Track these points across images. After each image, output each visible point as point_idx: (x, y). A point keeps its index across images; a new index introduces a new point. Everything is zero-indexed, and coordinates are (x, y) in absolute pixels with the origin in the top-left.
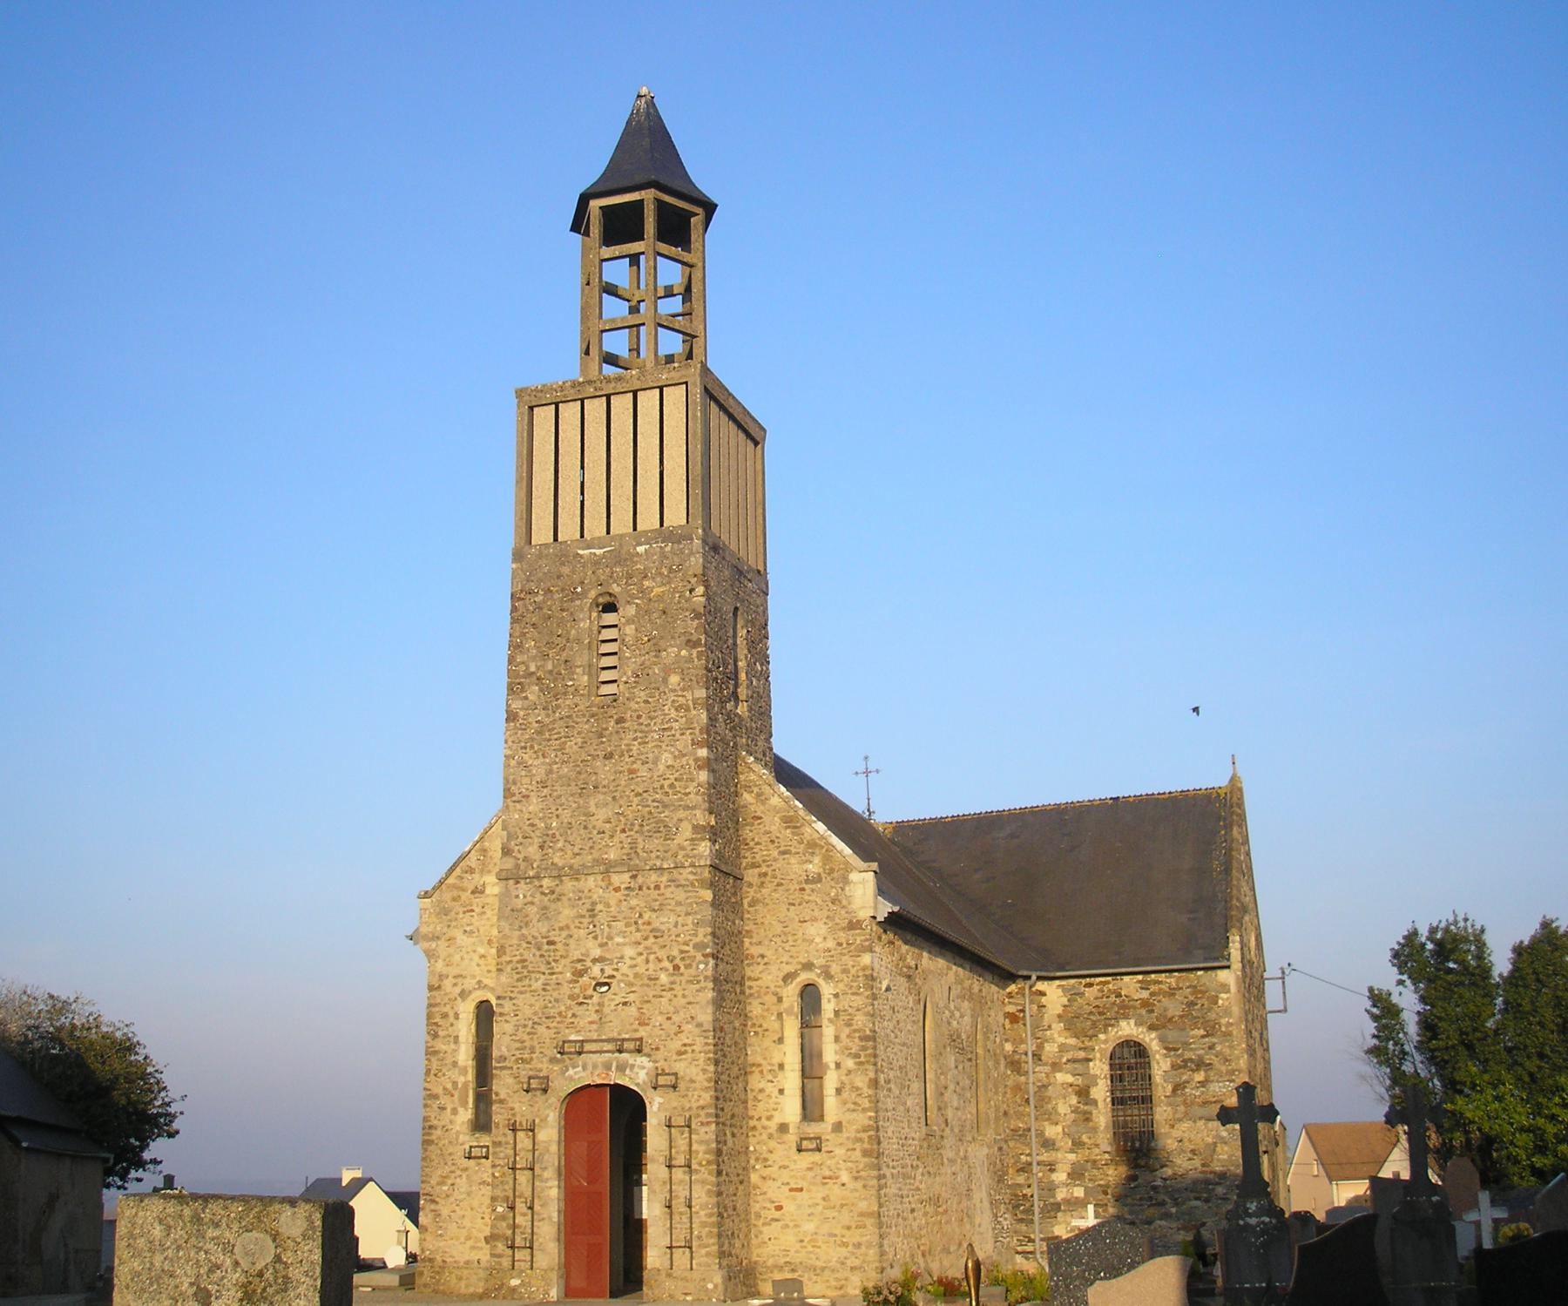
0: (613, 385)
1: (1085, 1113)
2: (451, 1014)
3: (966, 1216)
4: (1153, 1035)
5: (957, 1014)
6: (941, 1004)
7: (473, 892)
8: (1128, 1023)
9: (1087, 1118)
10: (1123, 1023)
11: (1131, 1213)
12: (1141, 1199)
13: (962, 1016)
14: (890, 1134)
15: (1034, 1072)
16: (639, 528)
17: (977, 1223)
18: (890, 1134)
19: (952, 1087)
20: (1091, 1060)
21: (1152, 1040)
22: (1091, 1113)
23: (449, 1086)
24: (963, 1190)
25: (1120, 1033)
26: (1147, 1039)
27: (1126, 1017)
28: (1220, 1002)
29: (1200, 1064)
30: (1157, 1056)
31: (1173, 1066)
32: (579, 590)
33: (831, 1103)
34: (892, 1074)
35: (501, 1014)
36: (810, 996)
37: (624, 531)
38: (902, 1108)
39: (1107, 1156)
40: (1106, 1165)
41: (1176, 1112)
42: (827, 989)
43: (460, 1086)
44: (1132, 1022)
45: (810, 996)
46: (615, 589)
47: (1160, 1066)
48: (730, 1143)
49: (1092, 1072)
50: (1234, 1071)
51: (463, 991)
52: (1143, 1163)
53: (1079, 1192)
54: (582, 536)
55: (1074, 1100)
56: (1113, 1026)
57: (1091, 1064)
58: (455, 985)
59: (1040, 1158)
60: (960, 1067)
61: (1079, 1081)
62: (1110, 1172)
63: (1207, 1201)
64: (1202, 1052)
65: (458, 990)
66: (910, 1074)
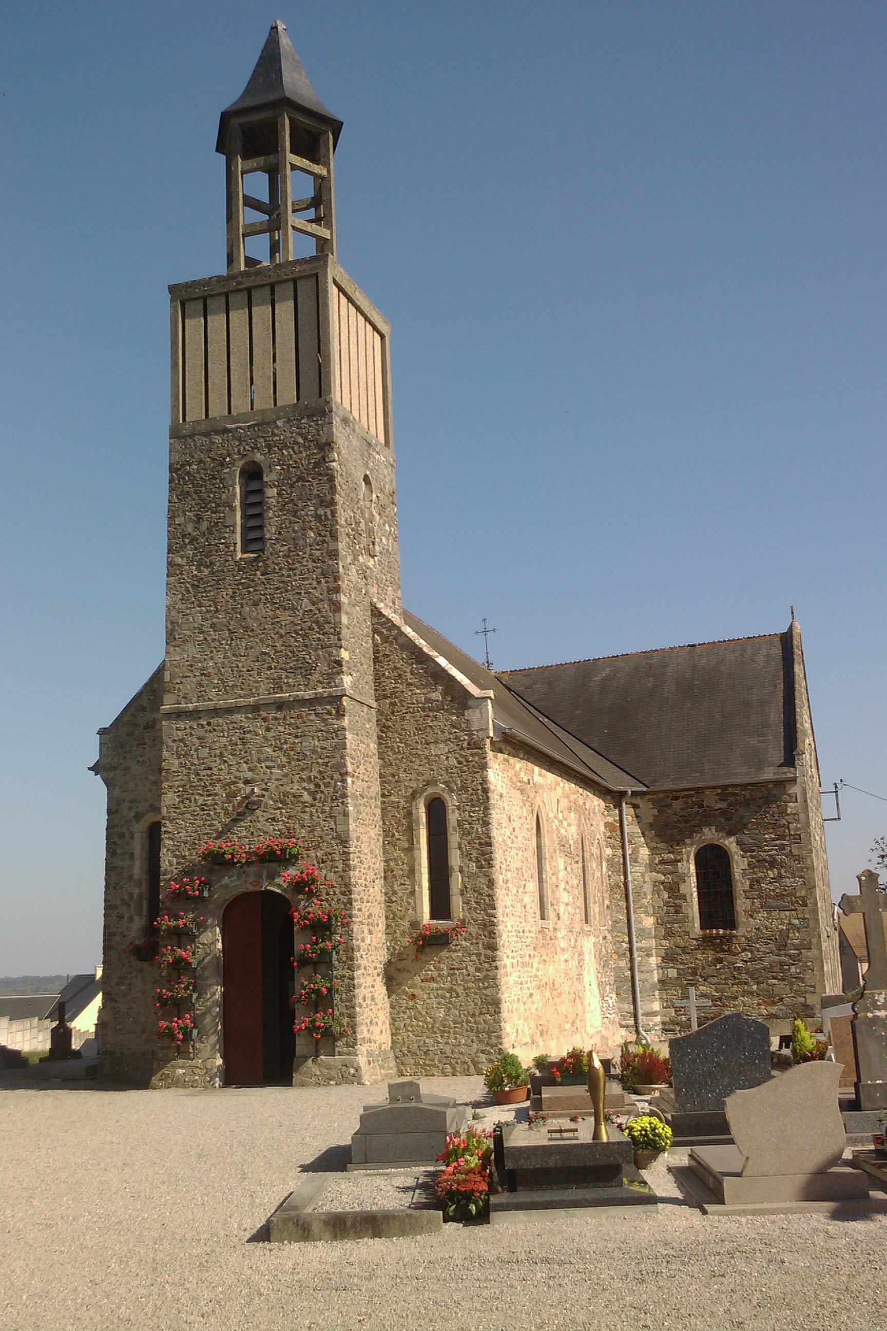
0: (253, 278)
1: (676, 906)
2: (127, 834)
3: (577, 997)
4: (732, 839)
5: (565, 824)
6: (551, 815)
7: (145, 728)
8: (710, 830)
9: (678, 910)
10: (706, 830)
11: (717, 990)
12: (725, 979)
13: (569, 825)
14: (509, 928)
15: (631, 872)
16: (279, 404)
17: (586, 1003)
18: (509, 928)
19: (562, 885)
20: (679, 861)
21: (731, 843)
22: (680, 907)
23: (126, 897)
24: (574, 973)
25: (703, 838)
26: (727, 842)
27: (709, 825)
28: (789, 811)
29: (773, 864)
30: (736, 857)
31: (749, 865)
32: (228, 459)
33: (457, 903)
34: (509, 874)
35: (166, 832)
36: (436, 809)
37: (266, 406)
38: (519, 905)
39: (695, 942)
40: (696, 949)
41: (753, 903)
42: (452, 801)
43: (135, 896)
44: (714, 830)
45: (436, 809)
46: (258, 457)
47: (739, 864)
48: (368, 941)
49: (680, 871)
50: (802, 868)
51: (137, 813)
52: (726, 948)
53: (673, 973)
54: (230, 412)
55: (666, 895)
56: (697, 832)
57: (679, 864)
58: (130, 808)
59: (639, 945)
60: (569, 869)
61: (670, 878)
62: (699, 956)
63: (783, 980)
64: (774, 852)
65: (132, 813)
66: (526, 875)
